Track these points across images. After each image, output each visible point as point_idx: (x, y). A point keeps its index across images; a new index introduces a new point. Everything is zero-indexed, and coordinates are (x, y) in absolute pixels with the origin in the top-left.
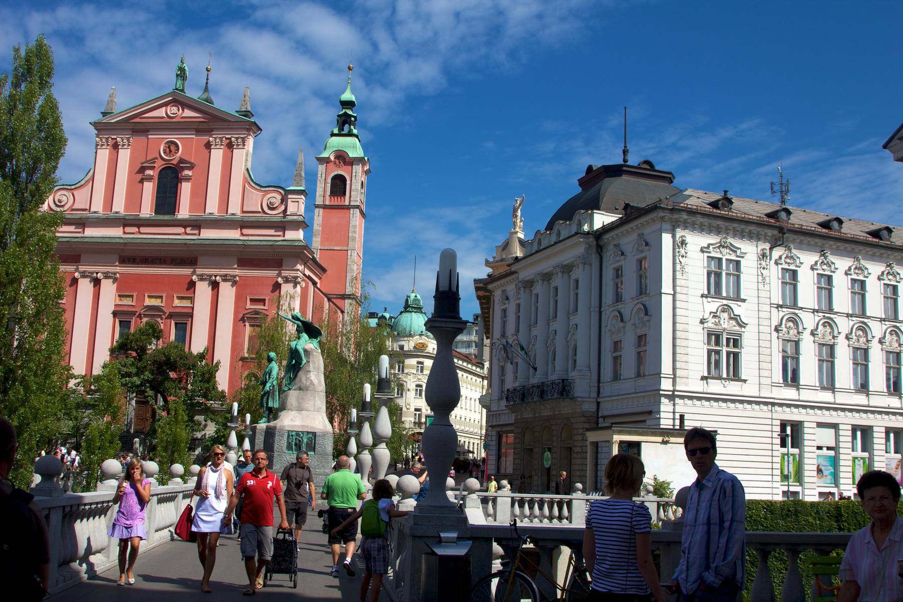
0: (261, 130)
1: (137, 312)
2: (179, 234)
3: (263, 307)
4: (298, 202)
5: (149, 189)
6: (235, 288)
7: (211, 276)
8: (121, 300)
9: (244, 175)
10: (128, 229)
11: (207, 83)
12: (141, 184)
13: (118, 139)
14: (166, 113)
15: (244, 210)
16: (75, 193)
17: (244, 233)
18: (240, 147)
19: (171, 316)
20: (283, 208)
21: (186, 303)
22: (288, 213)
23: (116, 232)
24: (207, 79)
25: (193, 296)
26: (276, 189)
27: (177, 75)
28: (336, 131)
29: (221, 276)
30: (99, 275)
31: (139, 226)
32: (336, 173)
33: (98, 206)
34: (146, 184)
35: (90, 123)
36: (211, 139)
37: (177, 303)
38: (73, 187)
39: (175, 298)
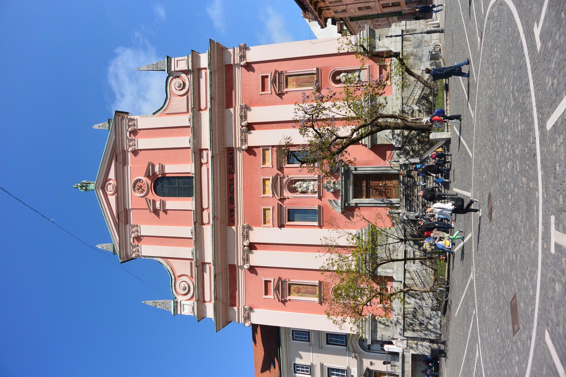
1: (278, 203)
2: (208, 169)
4: (177, 61)
6: (251, 108)
7: (242, 132)
8: (269, 222)
9: (159, 116)
10: (205, 220)
12: (168, 212)
15: (186, 111)
16: (178, 274)
17: (205, 107)
18: (136, 123)
19: (281, 169)
20: (183, 75)
21: (269, 154)
22: (186, 68)
23: (208, 231)
25: (261, 149)
26: (168, 85)
29: (242, 121)
30: (245, 244)
33: (187, 251)
34: (167, 207)
36: (130, 150)
37: (268, 164)
39: (264, 166)
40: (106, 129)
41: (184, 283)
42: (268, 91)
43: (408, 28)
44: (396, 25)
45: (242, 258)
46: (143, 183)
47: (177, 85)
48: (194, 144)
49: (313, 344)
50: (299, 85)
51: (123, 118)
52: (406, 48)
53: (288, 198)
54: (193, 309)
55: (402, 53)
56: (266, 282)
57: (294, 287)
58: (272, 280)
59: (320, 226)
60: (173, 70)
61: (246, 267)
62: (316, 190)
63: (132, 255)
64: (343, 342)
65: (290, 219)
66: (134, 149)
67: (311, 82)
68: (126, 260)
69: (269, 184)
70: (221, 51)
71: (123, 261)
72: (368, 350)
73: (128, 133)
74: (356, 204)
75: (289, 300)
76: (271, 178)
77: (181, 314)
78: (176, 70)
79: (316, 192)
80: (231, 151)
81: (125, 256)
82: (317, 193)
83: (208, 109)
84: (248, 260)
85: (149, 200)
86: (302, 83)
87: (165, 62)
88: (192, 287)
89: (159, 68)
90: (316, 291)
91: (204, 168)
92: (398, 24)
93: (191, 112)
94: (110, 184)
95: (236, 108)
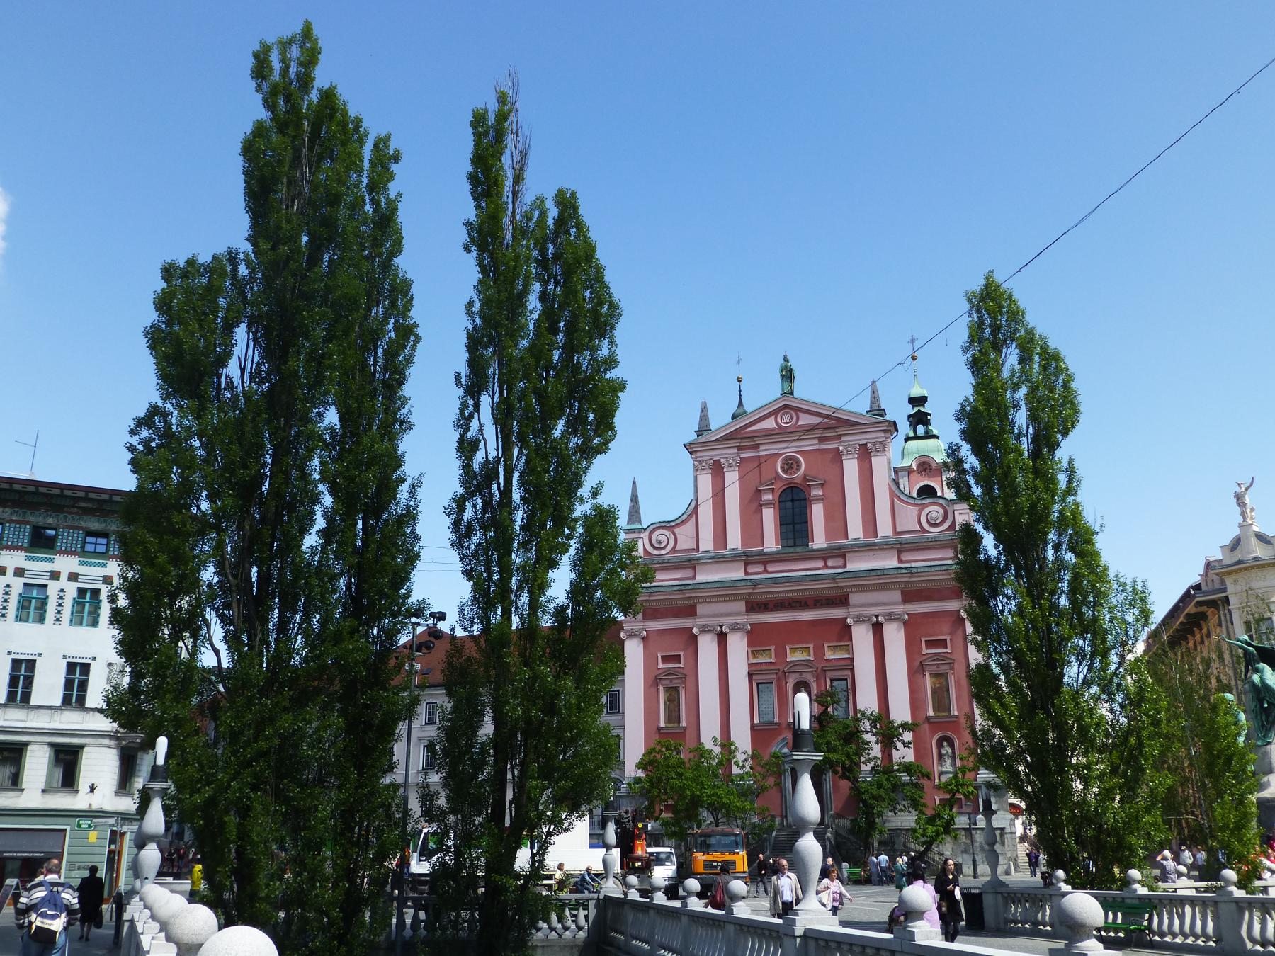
1: (779, 670)
3: (944, 650)
5: (769, 517)
7: (869, 618)
8: (754, 657)
11: (740, 396)
13: (722, 460)
14: (777, 423)
15: (898, 530)
24: (740, 391)
27: (783, 377)
28: (911, 434)
31: (765, 563)
32: (922, 484)
36: (841, 448)
38: (673, 524)
47: (934, 515)
48: (852, 546)
50: (934, 692)
51: (885, 431)
53: (786, 683)
56: (676, 659)
58: (681, 666)
65: (760, 686)
67: (938, 707)
73: (864, 442)
80: (844, 600)
88: (663, 552)
91: (821, 564)
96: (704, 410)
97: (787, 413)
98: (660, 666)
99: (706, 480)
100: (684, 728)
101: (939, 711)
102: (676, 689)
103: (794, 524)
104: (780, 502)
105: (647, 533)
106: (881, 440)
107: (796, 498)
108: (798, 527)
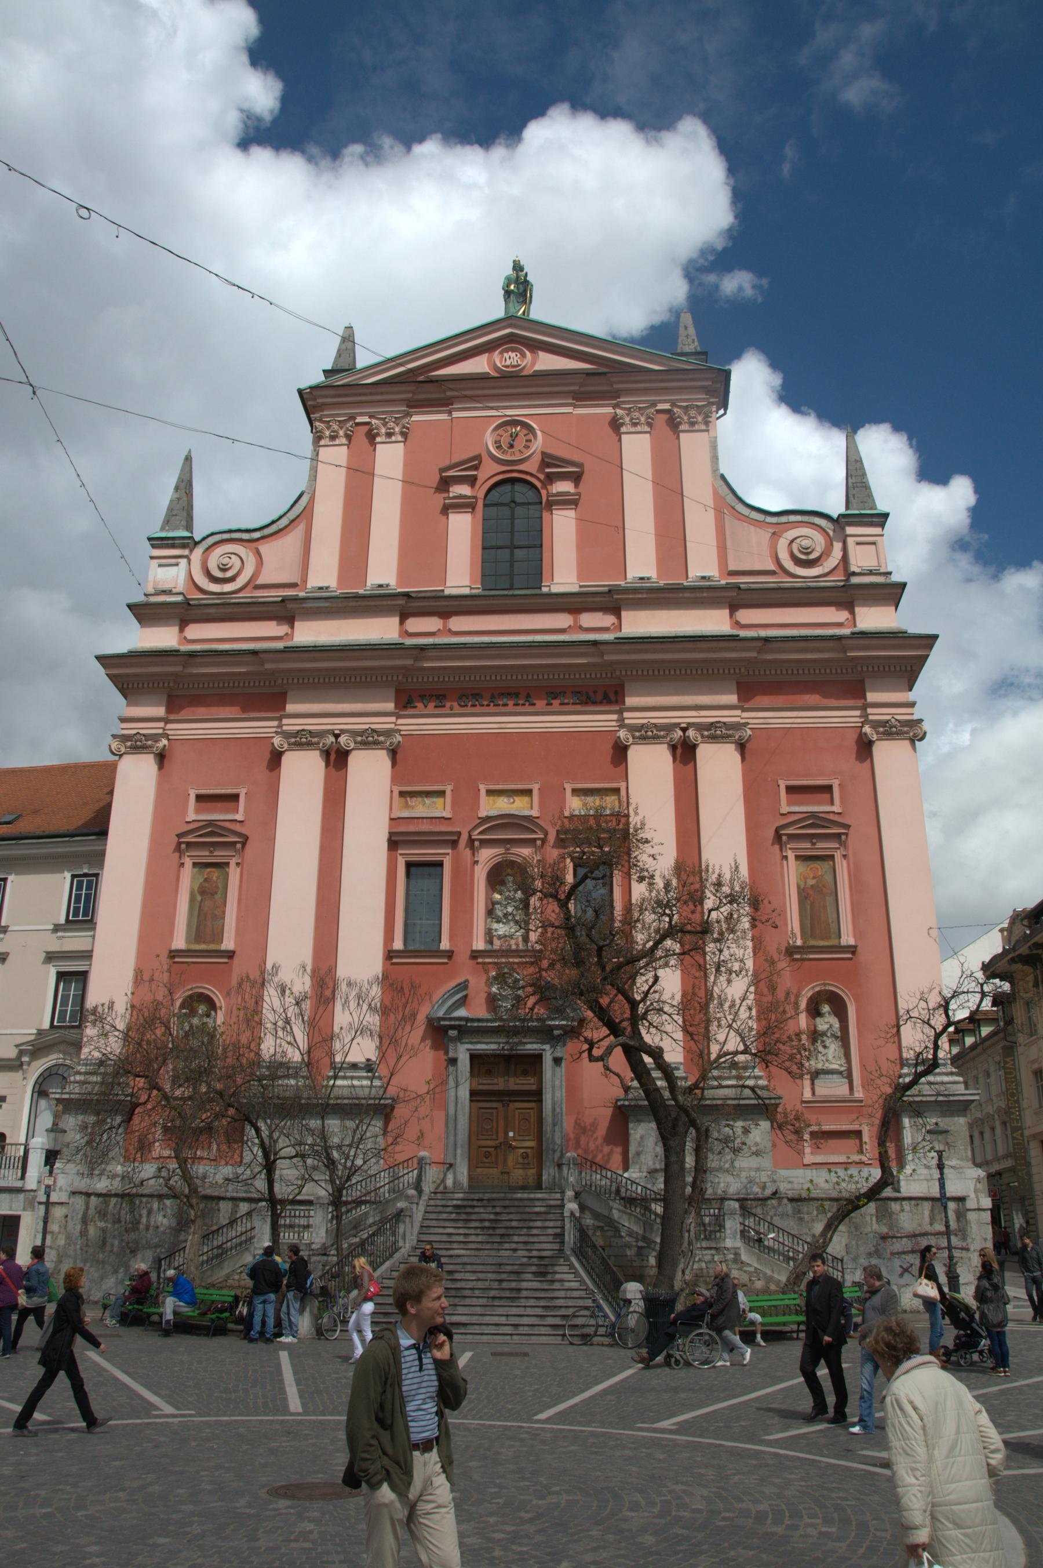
0: (726, 409)
1: (459, 834)
4: (874, 543)
7: (669, 728)
8: (407, 806)
10: (415, 624)
15: (732, 567)
16: (264, 548)
17: (743, 622)
26: (806, 518)
29: (700, 727)
30: (342, 739)
31: (445, 614)
35: (300, 392)
38: (257, 535)
39: (568, 792)
40: (680, 346)
41: (238, 563)
42: (789, 804)
43: (971, 1216)
44: (978, 1180)
45: (303, 730)
46: (523, 450)
47: (805, 543)
48: (635, 590)
49: (60, 934)
50: (804, 895)
51: (707, 391)
52: (911, 1211)
54: (164, 592)
55: (896, 1199)
57: (218, 878)
58: (239, 817)
59: (390, 955)
60: (850, 530)
61: (277, 741)
62: (497, 944)
63: (321, 421)
64: (62, 1018)
65: (413, 870)
66: (622, 424)
67: (812, 929)
68: (310, 403)
69: (519, 806)
70: (903, 668)
71: (305, 396)
72: (36, 1089)
73: (666, 406)
74: (453, 1061)
75: (183, 864)
76: (535, 813)
77: (152, 558)
78: (850, 541)
79: (491, 942)
80: (613, 698)
81: (320, 401)
82: (489, 947)
83: (735, 632)
84: (299, 746)
85: (476, 468)
86: (812, 904)
87: (871, 509)
88: (228, 587)
89: (855, 492)
90: (204, 942)
91: (562, 620)
92: (983, 1186)
93: (727, 584)
94: (523, 356)
95: (738, 712)
96: (348, 339)
97: (513, 350)
98: (191, 816)
99: (336, 454)
100: (230, 955)
101: (813, 936)
102: (222, 866)
103: (513, 547)
104: (485, 505)
105: (198, 552)
106: (699, 404)
107: (519, 499)
108: (519, 554)
